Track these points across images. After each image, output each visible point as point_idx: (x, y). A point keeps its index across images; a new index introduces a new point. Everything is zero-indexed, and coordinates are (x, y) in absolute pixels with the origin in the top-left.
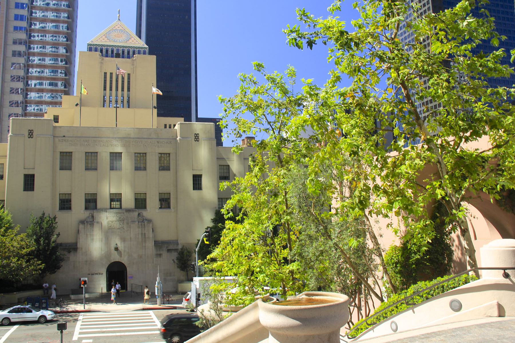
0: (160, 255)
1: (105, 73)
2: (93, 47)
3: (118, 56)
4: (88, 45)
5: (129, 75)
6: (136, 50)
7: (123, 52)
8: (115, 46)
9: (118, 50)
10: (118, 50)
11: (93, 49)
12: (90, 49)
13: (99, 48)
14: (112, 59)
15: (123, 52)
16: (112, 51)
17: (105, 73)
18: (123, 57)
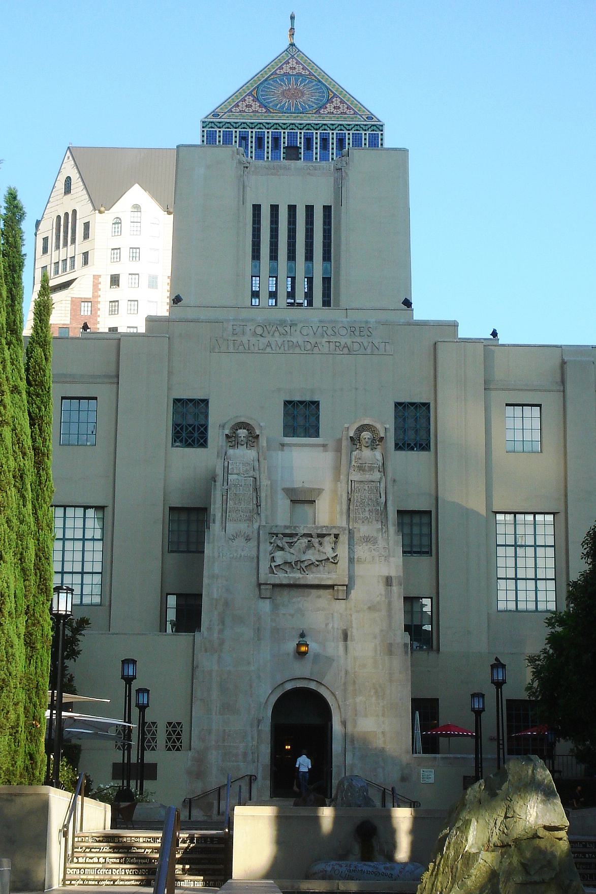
0: (375, 638)
1: (257, 208)
2: (220, 133)
3: (292, 152)
4: (205, 124)
5: (327, 209)
6: (349, 136)
7: (309, 141)
8: (284, 126)
9: (292, 136)
10: (292, 136)
11: (219, 138)
12: (210, 138)
13: (236, 133)
14: (276, 163)
15: (309, 141)
16: (276, 140)
17: (257, 208)
18: (308, 158)
